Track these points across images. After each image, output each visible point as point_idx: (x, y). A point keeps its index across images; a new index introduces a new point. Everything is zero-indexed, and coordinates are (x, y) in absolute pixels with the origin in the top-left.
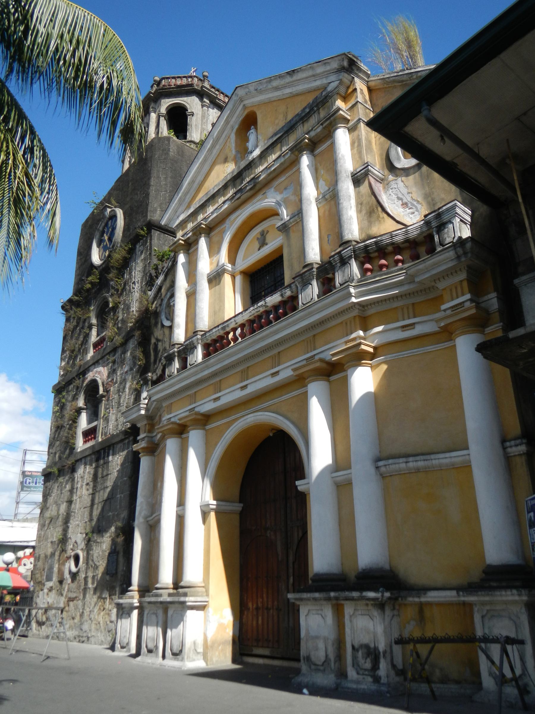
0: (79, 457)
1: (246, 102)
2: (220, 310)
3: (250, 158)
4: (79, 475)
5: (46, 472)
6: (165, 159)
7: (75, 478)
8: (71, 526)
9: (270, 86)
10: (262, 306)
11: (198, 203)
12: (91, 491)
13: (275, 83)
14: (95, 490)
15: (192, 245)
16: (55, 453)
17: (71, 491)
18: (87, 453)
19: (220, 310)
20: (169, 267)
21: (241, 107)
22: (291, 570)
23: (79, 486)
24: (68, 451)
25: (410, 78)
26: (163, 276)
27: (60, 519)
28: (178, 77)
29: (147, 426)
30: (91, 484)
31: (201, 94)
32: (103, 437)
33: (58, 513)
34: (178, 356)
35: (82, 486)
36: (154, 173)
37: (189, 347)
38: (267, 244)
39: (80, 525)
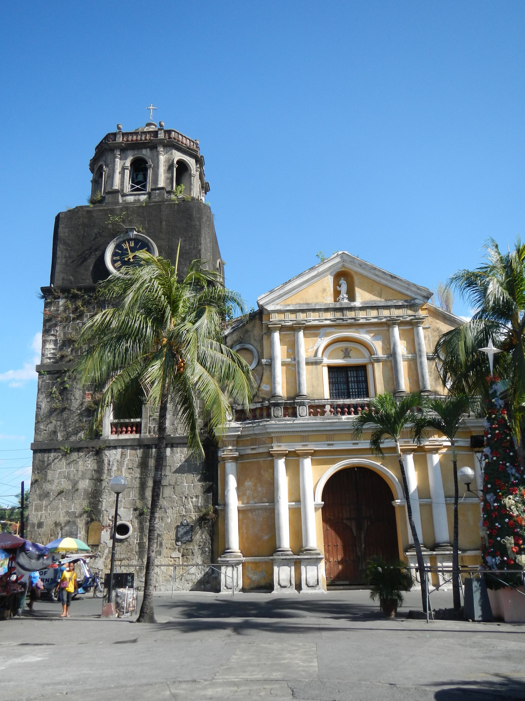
0: (112, 444)
1: (344, 263)
2: (318, 385)
3: (353, 304)
4: (111, 459)
5: (40, 448)
6: (208, 225)
7: (103, 460)
8: (105, 500)
9: (373, 271)
10: (366, 401)
11: (299, 307)
12: (139, 476)
13: (377, 273)
14: (146, 475)
15: (283, 329)
16: (55, 432)
17: (99, 471)
18: (129, 444)
19: (318, 385)
20: (239, 326)
21: (341, 265)
22: (363, 541)
23: (115, 468)
24: (82, 435)
25: (450, 318)
26: (232, 330)
27: (81, 493)
28: (185, 137)
29: (235, 442)
30: (138, 470)
31: (199, 161)
32: (152, 434)
33: (73, 487)
34: (284, 405)
35: (119, 469)
36: (203, 235)
37: (299, 404)
38: (350, 357)
39: (123, 501)
